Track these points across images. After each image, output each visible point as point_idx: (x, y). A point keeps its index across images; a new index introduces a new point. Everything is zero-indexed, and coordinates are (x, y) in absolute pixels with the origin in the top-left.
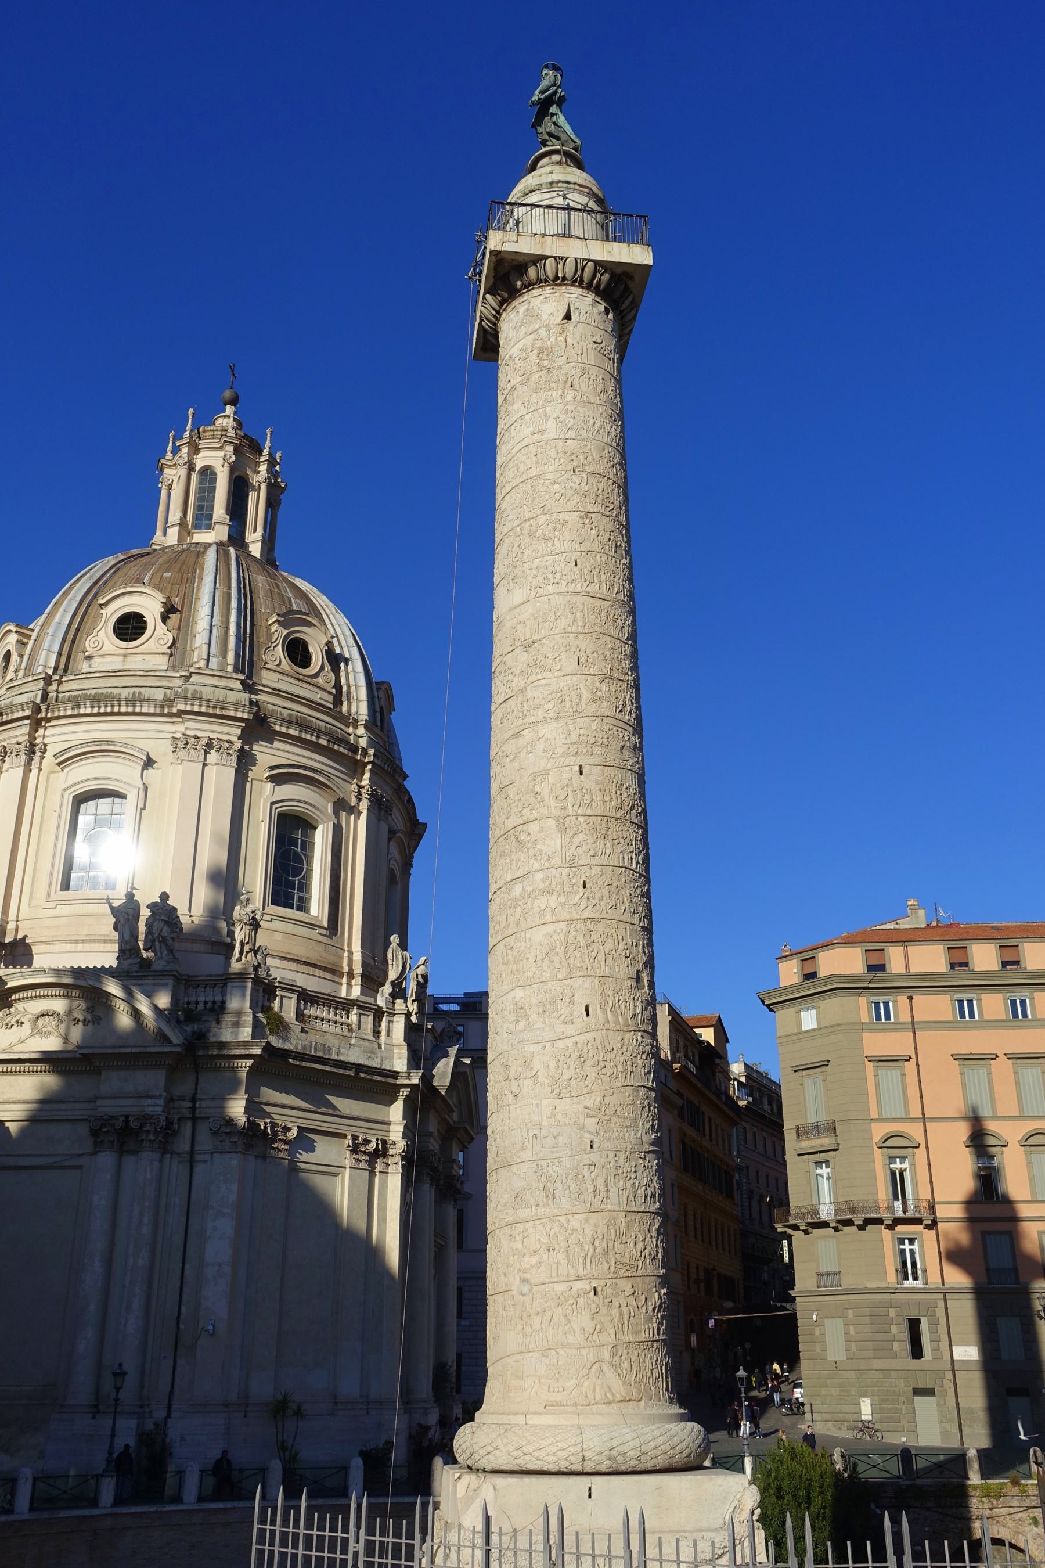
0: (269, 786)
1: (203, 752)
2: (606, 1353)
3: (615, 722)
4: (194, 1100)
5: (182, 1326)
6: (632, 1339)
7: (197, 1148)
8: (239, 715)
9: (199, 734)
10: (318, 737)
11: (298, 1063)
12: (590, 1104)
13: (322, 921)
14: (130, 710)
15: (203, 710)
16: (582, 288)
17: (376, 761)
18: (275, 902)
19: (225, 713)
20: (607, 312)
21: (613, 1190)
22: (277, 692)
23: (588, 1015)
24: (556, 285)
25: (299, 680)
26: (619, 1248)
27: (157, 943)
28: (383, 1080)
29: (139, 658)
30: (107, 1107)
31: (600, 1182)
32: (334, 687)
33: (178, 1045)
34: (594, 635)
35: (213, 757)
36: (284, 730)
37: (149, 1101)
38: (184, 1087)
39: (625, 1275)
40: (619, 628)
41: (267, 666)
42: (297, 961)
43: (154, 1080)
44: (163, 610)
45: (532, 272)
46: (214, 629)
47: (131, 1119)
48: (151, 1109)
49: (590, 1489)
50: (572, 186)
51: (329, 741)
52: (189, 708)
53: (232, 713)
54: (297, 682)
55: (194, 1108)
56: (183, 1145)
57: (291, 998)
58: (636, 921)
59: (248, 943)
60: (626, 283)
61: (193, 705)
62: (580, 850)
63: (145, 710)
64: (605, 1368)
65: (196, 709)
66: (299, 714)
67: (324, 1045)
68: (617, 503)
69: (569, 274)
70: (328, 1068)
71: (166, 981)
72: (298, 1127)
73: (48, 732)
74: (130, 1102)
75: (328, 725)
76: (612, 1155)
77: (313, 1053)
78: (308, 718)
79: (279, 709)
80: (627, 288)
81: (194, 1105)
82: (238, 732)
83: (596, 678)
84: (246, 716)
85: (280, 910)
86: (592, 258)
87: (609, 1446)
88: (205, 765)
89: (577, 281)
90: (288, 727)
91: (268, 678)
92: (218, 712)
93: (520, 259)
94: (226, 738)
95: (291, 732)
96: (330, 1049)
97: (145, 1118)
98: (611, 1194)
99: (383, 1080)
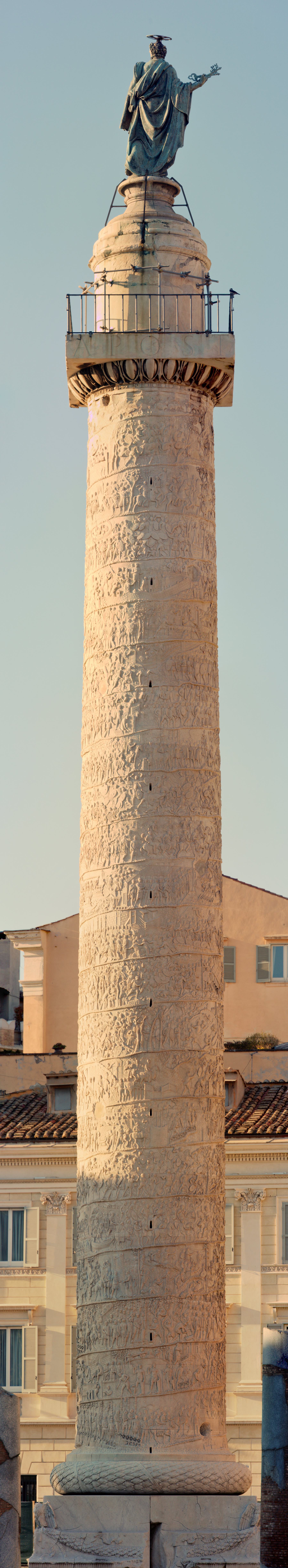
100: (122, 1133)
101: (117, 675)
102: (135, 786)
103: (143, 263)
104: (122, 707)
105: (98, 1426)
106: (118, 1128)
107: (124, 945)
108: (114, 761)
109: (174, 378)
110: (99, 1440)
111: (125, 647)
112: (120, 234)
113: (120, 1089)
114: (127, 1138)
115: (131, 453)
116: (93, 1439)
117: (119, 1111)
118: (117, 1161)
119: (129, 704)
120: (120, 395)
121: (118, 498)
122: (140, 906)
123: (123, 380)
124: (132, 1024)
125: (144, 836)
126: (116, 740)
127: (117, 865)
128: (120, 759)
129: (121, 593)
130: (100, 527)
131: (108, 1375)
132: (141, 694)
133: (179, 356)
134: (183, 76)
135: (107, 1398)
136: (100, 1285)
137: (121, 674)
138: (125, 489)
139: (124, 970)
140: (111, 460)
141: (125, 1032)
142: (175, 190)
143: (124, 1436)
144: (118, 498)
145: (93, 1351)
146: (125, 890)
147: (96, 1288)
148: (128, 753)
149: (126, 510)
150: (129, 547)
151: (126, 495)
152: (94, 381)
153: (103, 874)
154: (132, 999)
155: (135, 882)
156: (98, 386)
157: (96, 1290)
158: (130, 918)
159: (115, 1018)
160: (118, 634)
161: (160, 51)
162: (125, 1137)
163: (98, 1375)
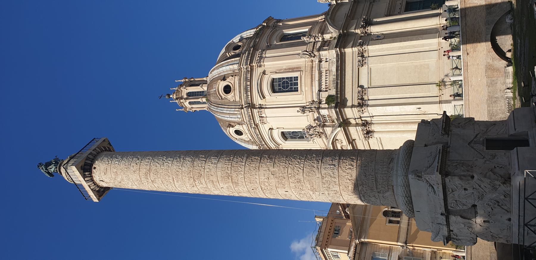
0: (267, 97)
1: (263, 118)
2: (381, 195)
4: (355, 119)
5: (419, 114)
6: (375, 187)
7: (369, 116)
8: (250, 111)
9: (259, 120)
10: (248, 85)
11: (339, 93)
12: (312, 193)
13: (299, 74)
14: (259, 135)
15: (252, 121)
16: (93, 178)
18: (297, 91)
19: (251, 115)
21: (334, 189)
22: (240, 98)
23: (288, 191)
24: (96, 183)
25: (235, 89)
27: (316, 131)
28: (339, 59)
29: (246, 131)
30: (362, 137)
31: (332, 192)
33: (341, 128)
34: (184, 182)
36: (250, 97)
37: (358, 130)
38: (353, 121)
39: (357, 187)
40: (179, 173)
41: (234, 100)
42: (312, 81)
43: (352, 130)
44: (231, 127)
45: (98, 189)
46: (231, 117)
47: (364, 133)
48: (360, 129)
49: (417, 211)
51: (248, 81)
52: (253, 124)
53: (250, 113)
54: (236, 90)
55: (358, 118)
56: (368, 119)
57: (322, 94)
58: (257, 173)
59: (309, 111)
60: (84, 166)
61: (252, 123)
62: (244, 190)
63: (258, 132)
64: (385, 195)
65: (253, 122)
67: (333, 81)
68: (145, 170)
69: (92, 183)
70: (339, 81)
71: (325, 129)
72: (358, 87)
74: (359, 133)
76: (324, 189)
77: (335, 85)
79: (245, 97)
80: (85, 165)
81: (357, 118)
83: (196, 183)
84: (250, 110)
85: (299, 89)
86: (84, 180)
87: (405, 205)
89: (92, 180)
90: (249, 96)
92: (251, 117)
93: (96, 194)
94: (258, 113)
95: (249, 94)
96: (334, 79)
97: (363, 130)
98: (335, 190)
99: (339, 59)
100: (283, 162)
102: (187, 158)
105: (385, 175)
106: (281, 164)
107: (227, 161)
108: (178, 165)
110: (391, 174)
113: (269, 163)
114: (285, 161)
116: (390, 178)
117: (276, 163)
118: (291, 165)
121: (117, 163)
122: (219, 157)
124: (251, 159)
125: (201, 156)
126: (172, 164)
127: (205, 163)
128: (178, 163)
131: (365, 170)
132: (165, 157)
135: (374, 170)
136: (332, 173)
137: (157, 162)
139: (235, 161)
141: (253, 161)
143: (390, 163)
146: (213, 161)
147: (332, 175)
150: (129, 160)
153: (206, 169)
154: (244, 159)
155: (212, 158)
157: (333, 175)
158: (221, 160)
159: (248, 164)
162: (284, 162)
163: (365, 175)
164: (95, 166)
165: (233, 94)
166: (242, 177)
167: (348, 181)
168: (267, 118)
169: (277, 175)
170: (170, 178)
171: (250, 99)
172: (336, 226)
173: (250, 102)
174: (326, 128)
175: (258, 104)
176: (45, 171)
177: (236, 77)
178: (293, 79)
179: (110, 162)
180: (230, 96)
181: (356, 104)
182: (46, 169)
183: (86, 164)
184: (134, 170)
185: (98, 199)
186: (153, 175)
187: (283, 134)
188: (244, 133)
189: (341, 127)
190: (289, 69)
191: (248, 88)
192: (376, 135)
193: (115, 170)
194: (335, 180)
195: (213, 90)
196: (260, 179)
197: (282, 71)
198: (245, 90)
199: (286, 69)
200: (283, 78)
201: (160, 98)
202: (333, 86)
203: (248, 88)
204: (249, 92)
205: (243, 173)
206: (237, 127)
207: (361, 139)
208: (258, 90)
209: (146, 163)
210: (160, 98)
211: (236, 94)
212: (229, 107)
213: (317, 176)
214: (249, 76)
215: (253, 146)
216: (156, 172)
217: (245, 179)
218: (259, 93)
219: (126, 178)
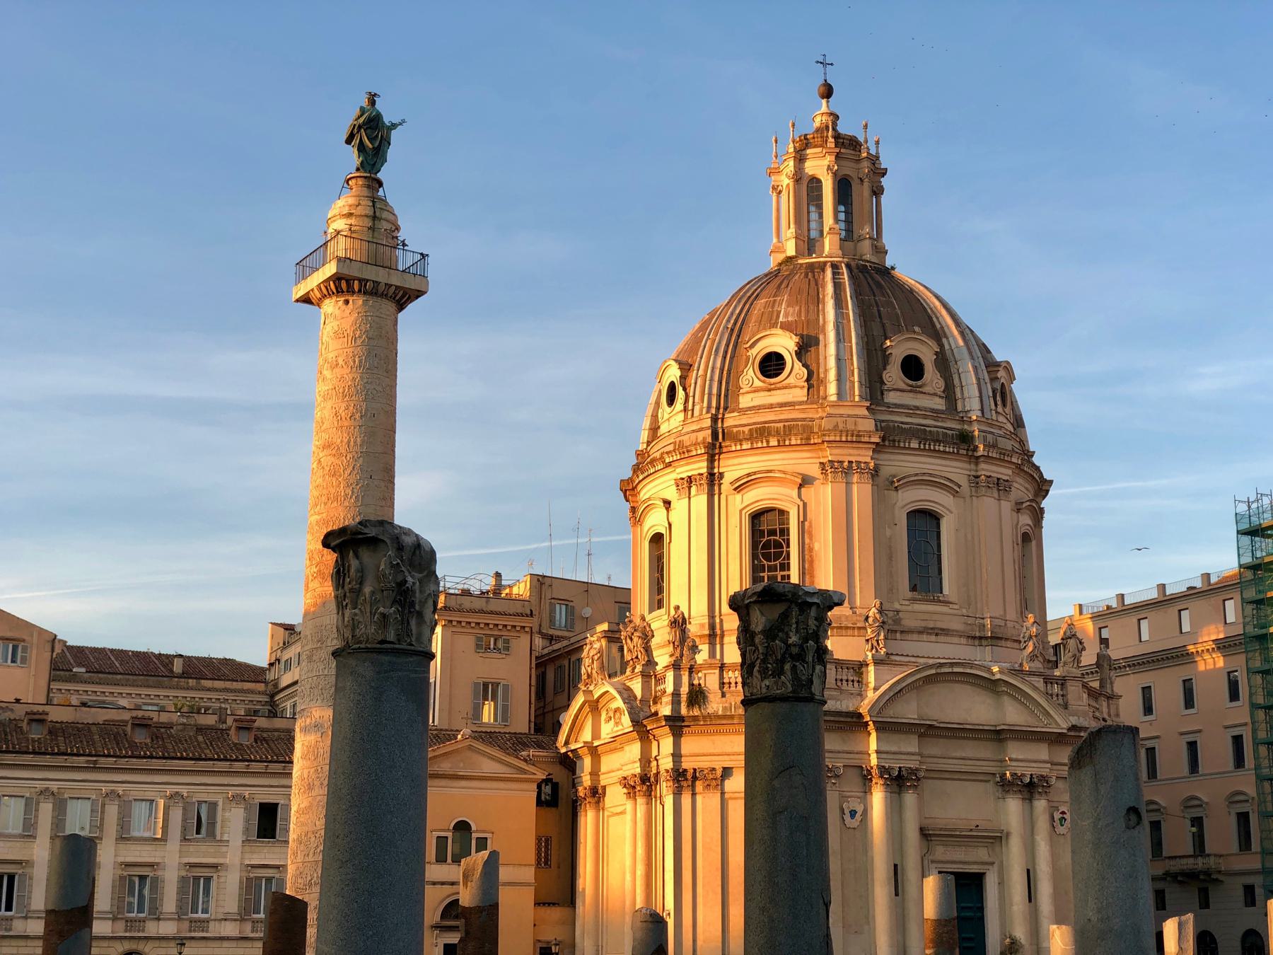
0: (738, 497)
3: (321, 589)
8: (699, 452)
17: (827, 439)
20: (347, 302)
25: (769, 390)
26: (300, 881)
32: (808, 380)
35: (693, 489)
36: (739, 448)
50: (332, 219)
51: (779, 441)
53: (694, 453)
54: (769, 393)
57: (714, 673)
66: (758, 426)
73: (642, 494)
75: (786, 424)
78: (766, 425)
79: (741, 429)
82: (705, 464)
86: (321, 281)
88: (690, 498)
90: (741, 445)
91: (745, 401)
95: (744, 447)
101: (351, 468)
103: (374, 225)
104: (353, 488)
109: (391, 297)
111: (356, 453)
112: (359, 204)
115: (364, 336)
119: (358, 488)
120: (356, 301)
121: (354, 362)
123: (363, 291)
128: (351, 520)
129: (355, 419)
130: (339, 377)
133: (399, 284)
134: (387, 120)
137: (353, 468)
138: (359, 357)
140: (350, 339)
142: (380, 184)
144: (354, 362)
145: (314, 891)
148: (357, 516)
149: (360, 369)
151: (360, 361)
152: (341, 288)
156: (343, 292)
160: (352, 443)
161: (372, 102)
164: (351, 302)
165: (757, 383)
166: (319, 672)
167: (309, 878)
168: (687, 499)
169: (321, 744)
170: (323, 505)
171: (733, 448)
172: (507, 641)
173: (725, 450)
174: (640, 684)
175: (721, 470)
176: (355, 125)
177: (806, 390)
178: (785, 573)
179: (359, 342)
180: (750, 376)
181: (684, 766)
182: (360, 127)
183: (349, 281)
184: (340, 412)
185: (297, 301)
186: (329, 464)
187: (657, 539)
188: (673, 407)
189: (633, 726)
190: (812, 562)
191: (762, 442)
192: (629, 806)
193: (341, 362)
194: (311, 855)
195: (783, 307)
196: (315, 709)
197: (807, 541)
198: (760, 428)
199: (811, 550)
200: (788, 546)
201: (818, 62)
202: (731, 704)
203: (762, 442)
204: (749, 446)
205: (326, 673)
206: (680, 393)
207: (624, 768)
208: (755, 473)
209: (352, 440)
210: (818, 62)
211: (756, 394)
212: (725, 372)
213: (317, 823)
214: (793, 442)
215: (647, 432)
216: (334, 472)
217: (316, 678)
218: (749, 475)
219: (326, 393)
